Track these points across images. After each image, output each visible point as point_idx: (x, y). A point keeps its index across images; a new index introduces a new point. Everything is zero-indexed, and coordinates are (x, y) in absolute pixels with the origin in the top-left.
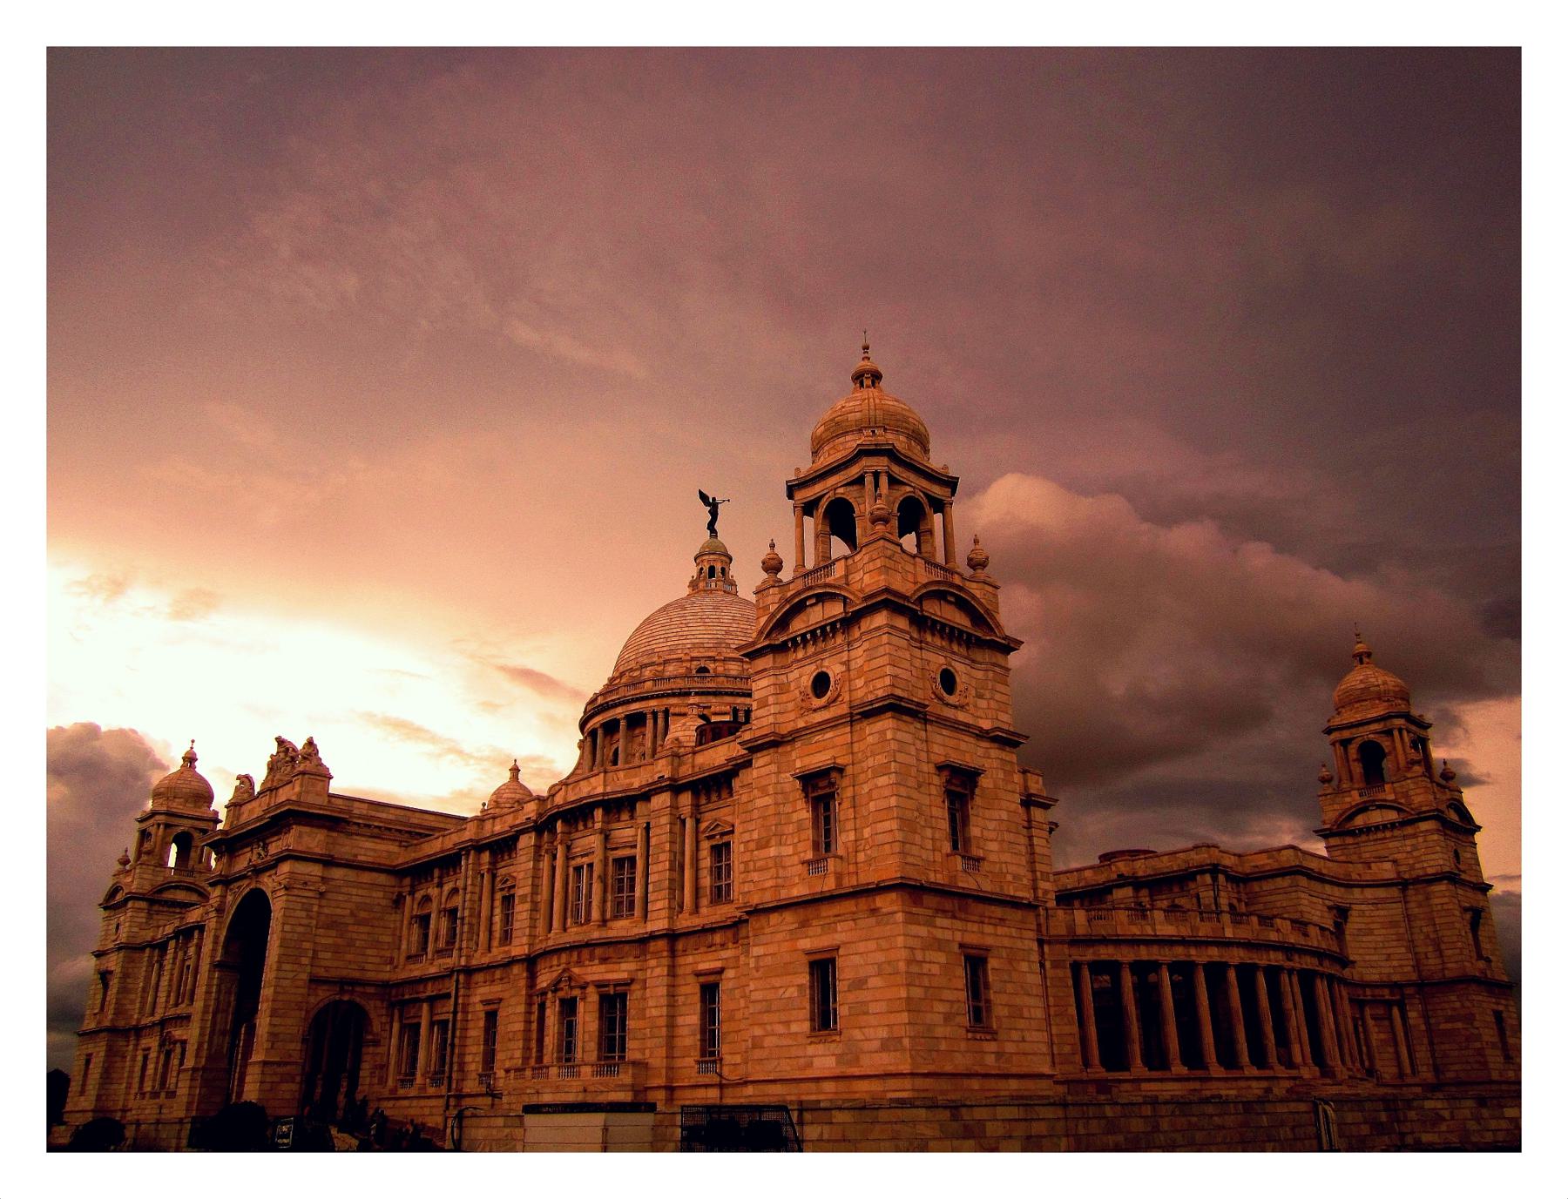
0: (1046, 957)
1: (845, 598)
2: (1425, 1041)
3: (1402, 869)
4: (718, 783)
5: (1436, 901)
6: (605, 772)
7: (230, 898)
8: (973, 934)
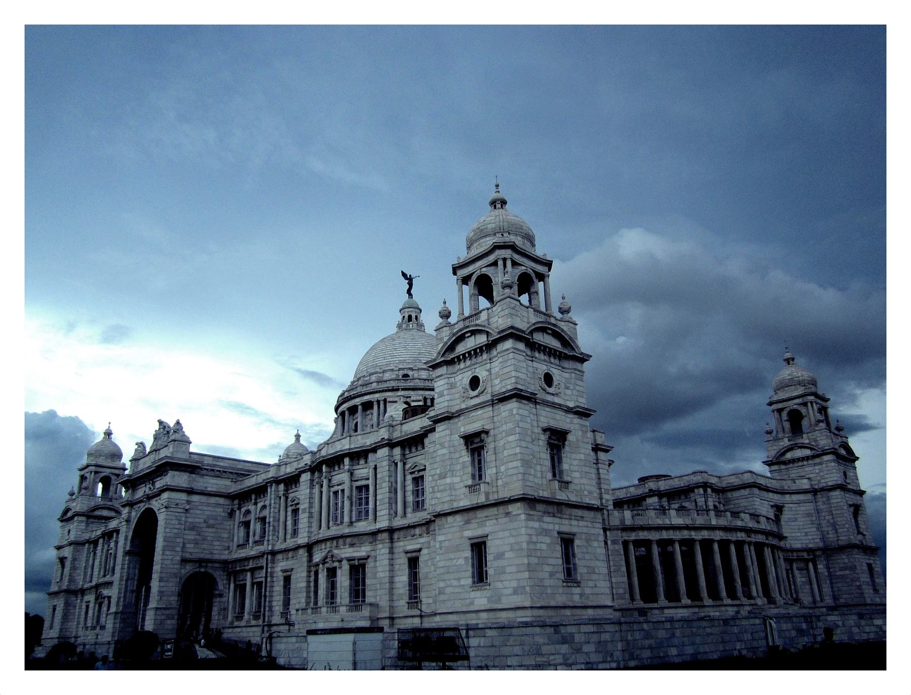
0: (608, 538)
2: (828, 582)
3: (814, 483)
4: (416, 442)
5: (834, 501)
6: (350, 436)
7: (133, 514)
8: (567, 526)
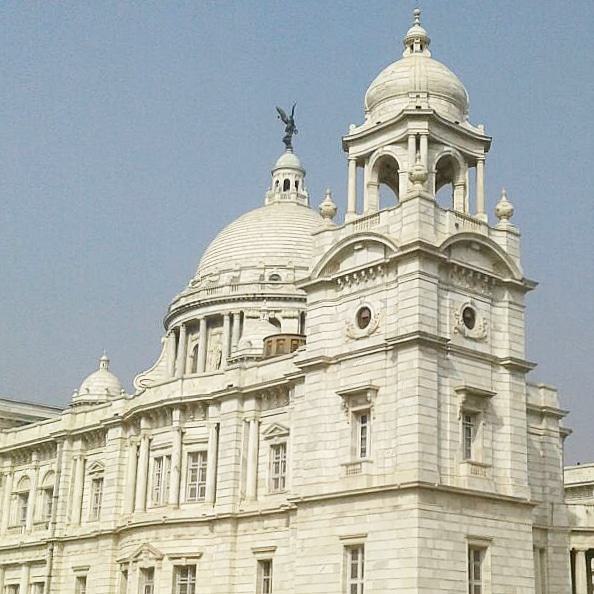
1: (385, 245)
4: (277, 393)
6: (183, 379)
